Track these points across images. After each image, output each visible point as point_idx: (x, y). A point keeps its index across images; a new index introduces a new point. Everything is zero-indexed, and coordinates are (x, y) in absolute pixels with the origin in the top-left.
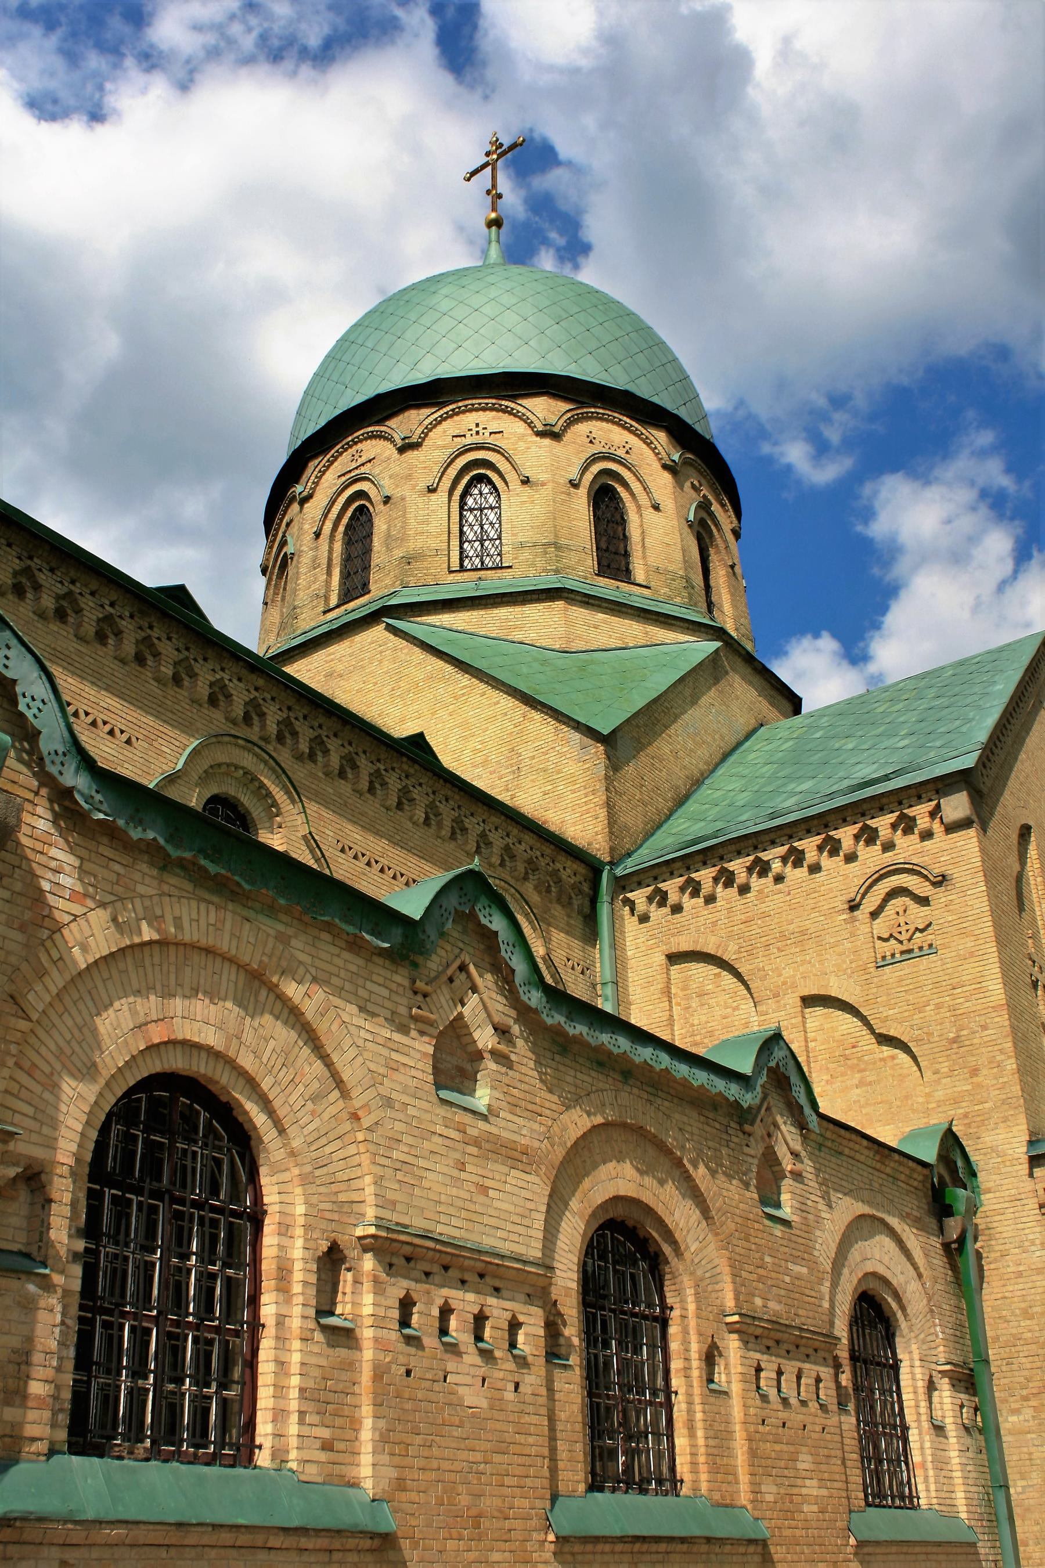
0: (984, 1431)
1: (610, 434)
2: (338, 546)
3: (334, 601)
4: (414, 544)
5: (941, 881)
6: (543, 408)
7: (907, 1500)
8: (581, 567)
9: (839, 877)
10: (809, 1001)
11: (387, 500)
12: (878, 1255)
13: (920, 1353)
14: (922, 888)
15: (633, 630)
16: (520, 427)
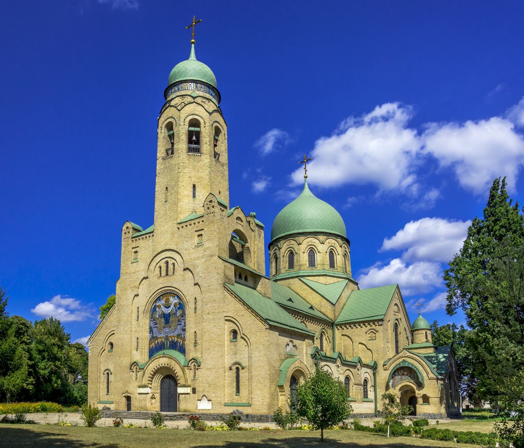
0: (375, 391)
1: (332, 241)
2: (287, 259)
3: (287, 268)
4: (302, 263)
5: (377, 331)
6: (322, 238)
7: (367, 397)
8: (327, 267)
9: (364, 329)
10: (360, 343)
11: (296, 253)
12: (367, 375)
13: (369, 385)
14: (375, 332)
15: (336, 280)
16: (318, 241)
